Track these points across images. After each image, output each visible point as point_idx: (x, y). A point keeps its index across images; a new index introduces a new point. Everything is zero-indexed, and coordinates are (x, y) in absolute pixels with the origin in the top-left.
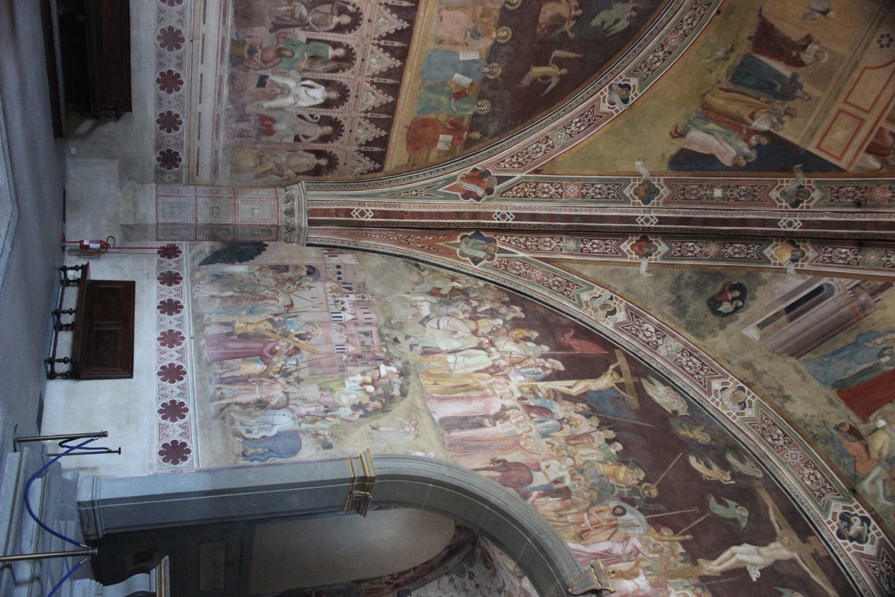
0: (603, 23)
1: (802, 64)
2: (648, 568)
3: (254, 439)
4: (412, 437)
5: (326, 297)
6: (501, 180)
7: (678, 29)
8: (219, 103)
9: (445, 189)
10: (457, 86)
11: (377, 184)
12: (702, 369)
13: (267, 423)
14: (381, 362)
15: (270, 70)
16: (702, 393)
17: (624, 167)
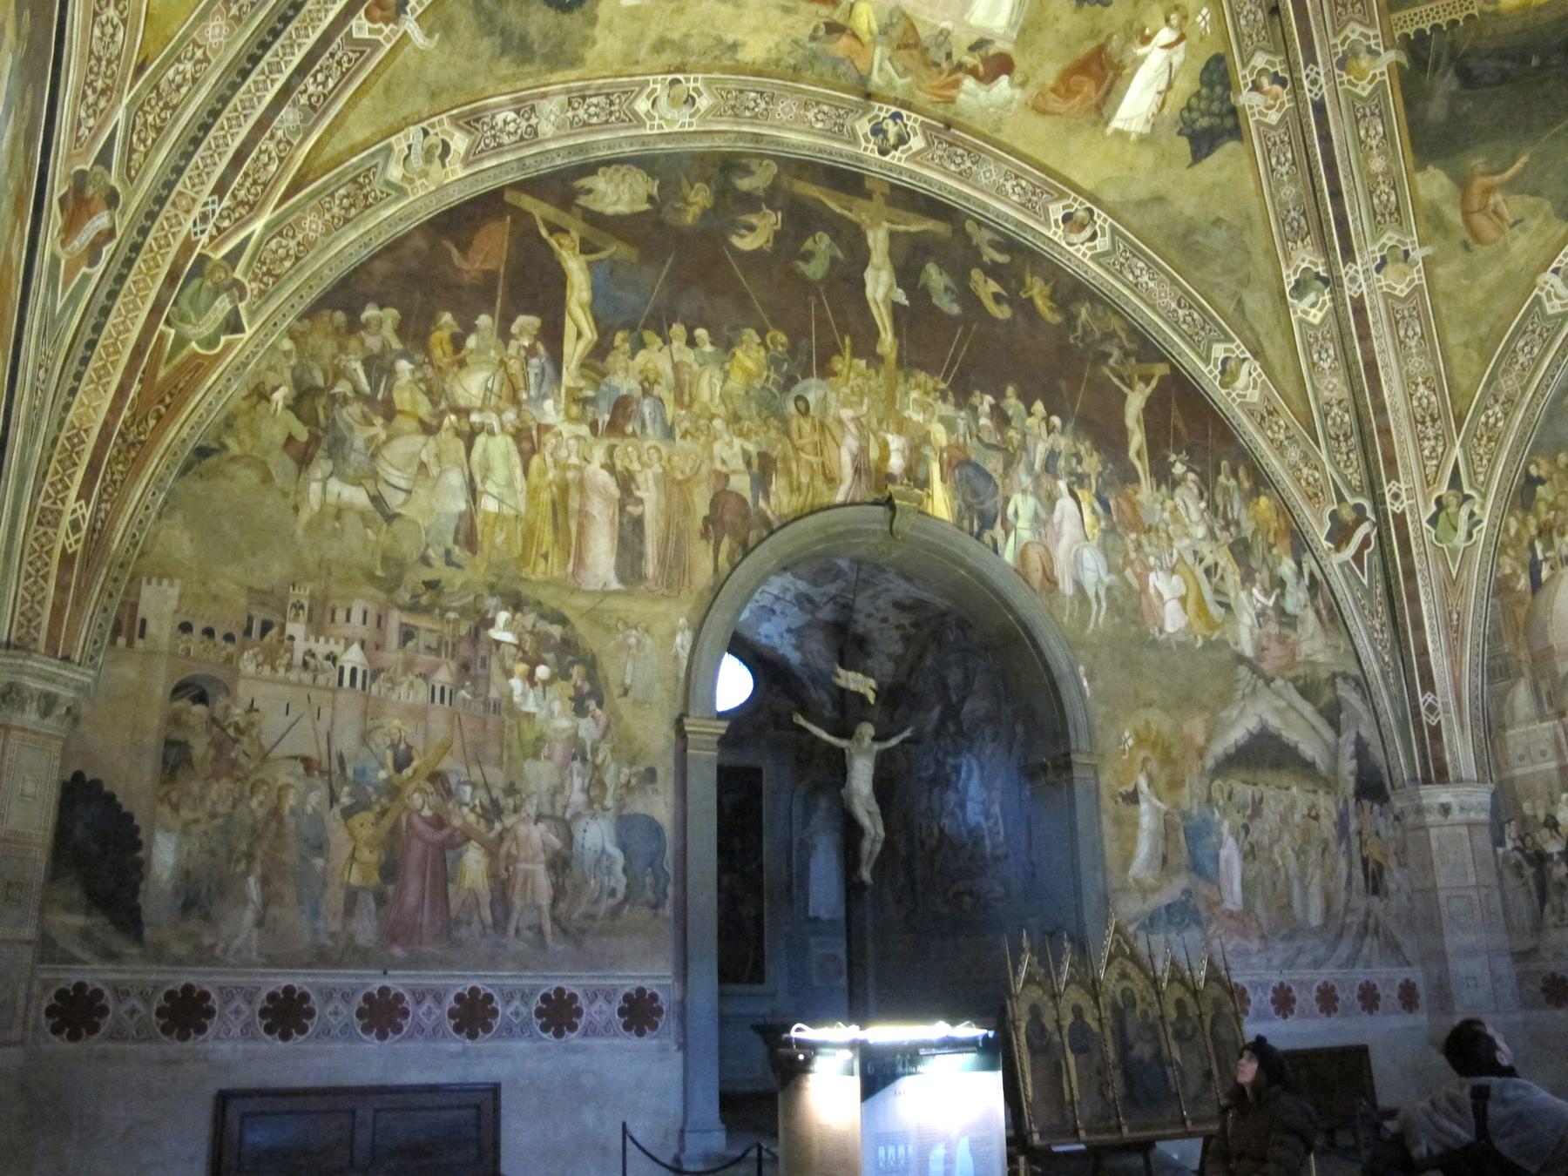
2: (880, 422)
3: (628, 886)
4: (648, 641)
6: (104, 158)
13: (598, 861)
14: (482, 632)
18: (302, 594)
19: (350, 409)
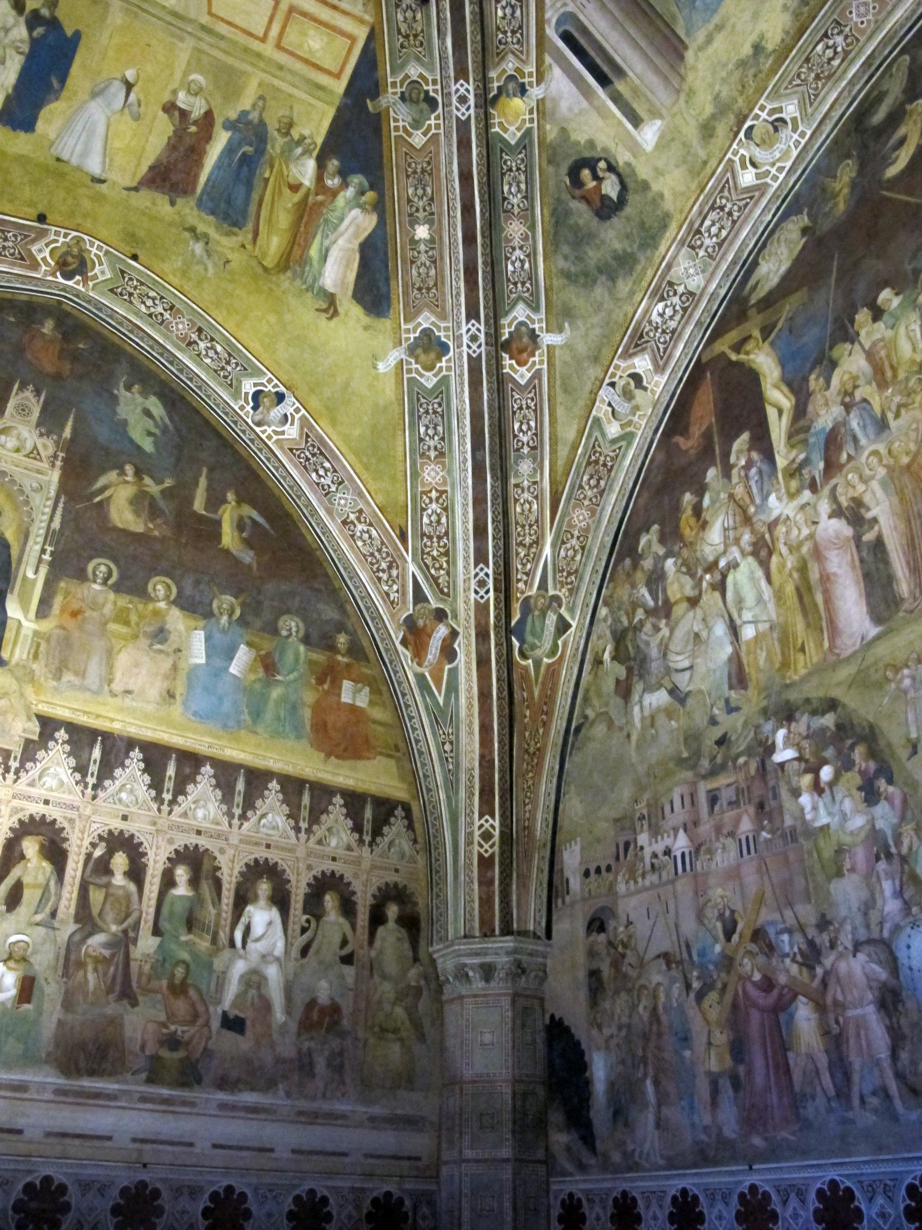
0: (150, 434)
1: (209, 115)
5: (646, 889)
6: (419, 596)
7: (163, 321)
8: (275, 1112)
9: (440, 692)
10: (252, 669)
11: (432, 813)
12: (722, 208)
14: (768, 763)
15: (211, 1009)
16: (764, 201)
17: (389, 390)
18: (642, 808)
19: (645, 629)
